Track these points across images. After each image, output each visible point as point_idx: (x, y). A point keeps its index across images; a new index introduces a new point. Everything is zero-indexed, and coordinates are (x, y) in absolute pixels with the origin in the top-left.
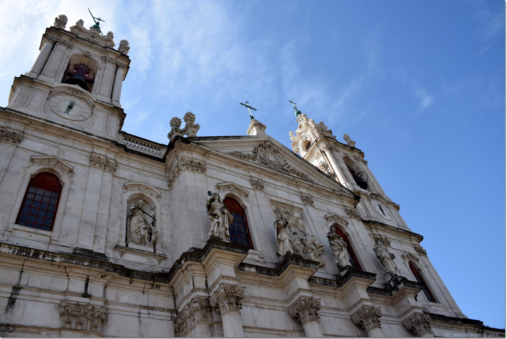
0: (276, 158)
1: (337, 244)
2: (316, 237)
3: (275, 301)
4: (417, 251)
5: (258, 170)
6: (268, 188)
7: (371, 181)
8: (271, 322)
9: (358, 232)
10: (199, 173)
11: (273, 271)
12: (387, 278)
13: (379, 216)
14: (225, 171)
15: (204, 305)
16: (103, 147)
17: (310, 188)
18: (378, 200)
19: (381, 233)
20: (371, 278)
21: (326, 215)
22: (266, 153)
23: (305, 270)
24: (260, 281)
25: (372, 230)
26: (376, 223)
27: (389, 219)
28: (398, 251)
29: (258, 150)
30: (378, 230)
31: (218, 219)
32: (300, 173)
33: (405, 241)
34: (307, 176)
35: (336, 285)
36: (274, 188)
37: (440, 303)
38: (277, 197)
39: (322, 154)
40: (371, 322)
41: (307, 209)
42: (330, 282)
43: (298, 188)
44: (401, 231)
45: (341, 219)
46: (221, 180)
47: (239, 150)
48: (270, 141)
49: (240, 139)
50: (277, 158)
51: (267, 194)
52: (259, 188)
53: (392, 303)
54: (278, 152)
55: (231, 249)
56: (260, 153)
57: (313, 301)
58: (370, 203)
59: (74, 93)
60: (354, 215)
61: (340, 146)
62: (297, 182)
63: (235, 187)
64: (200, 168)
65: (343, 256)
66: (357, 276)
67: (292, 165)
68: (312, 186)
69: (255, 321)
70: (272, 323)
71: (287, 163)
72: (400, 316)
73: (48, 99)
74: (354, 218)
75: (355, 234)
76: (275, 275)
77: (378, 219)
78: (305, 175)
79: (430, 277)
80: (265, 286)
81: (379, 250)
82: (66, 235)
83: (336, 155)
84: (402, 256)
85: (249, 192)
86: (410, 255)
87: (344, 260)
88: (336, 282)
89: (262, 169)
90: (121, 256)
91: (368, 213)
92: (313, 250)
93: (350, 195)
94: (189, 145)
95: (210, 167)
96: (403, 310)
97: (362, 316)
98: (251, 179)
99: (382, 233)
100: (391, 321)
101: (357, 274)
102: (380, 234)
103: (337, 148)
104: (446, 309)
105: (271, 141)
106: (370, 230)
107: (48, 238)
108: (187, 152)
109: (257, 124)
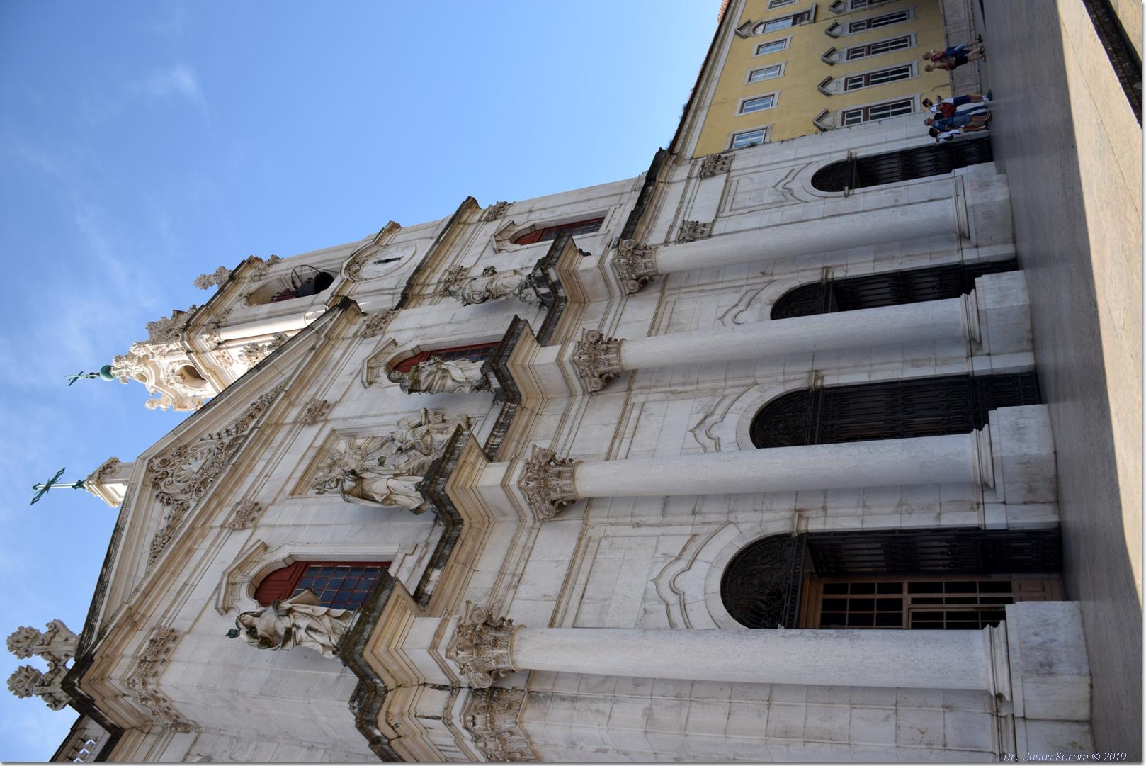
0: (199, 456)
1: (431, 377)
2: (403, 419)
3: (513, 544)
4: (495, 219)
5: (213, 506)
6: (263, 493)
7: (319, 262)
8: (555, 564)
10: (176, 648)
11: (449, 532)
12: (529, 296)
13: (399, 272)
14: (191, 583)
15: (484, 704)
17: (292, 399)
18: (365, 261)
19: (435, 278)
20: (519, 329)
21: (362, 382)
22: (178, 476)
23: (465, 462)
24: (465, 565)
25: (423, 295)
26: (412, 282)
27: (413, 252)
28: (482, 257)
29: (165, 493)
30: (426, 283)
31: (299, 628)
32: (251, 411)
33: (467, 236)
34: (262, 396)
35: (516, 405)
36: (266, 478)
37: (607, 211)
38: (289, 478)
39: (224, 349)
40: (607, 356)
41: (336, 420)
42: (506, 416)
43: (283, 425)
44: (444, 236)
45: (381, 352)
46: (210, 598)
47: (150, 538)
48: (153, 458)
49: (123, 529)
50: (200, 453)
51: (275, 499)
52: (256, 515)
53: (581, 303)
54: (185, 447)
55: (376, 614)
56: (175, 490)
57: (534, 462)
58: (366, 279)
60: (380, 322)
61: (217, 303)
62: (268, 425)
63: (237, 570)
64: (164, 643)
65: (460, 372)
66: (508, 356)
67: (225, 424)
68: (288, 394)
69: (546, 598)
70: (557, 561)
71: (219, 434)
72: (611, 297)
74: (387, 323)
75: (421, 332)
76: (460, 530)
77: (404, 274)
78: (259, 401)
79: (553, 211)
80: (478, 557)
81: (468, 294)
83: (237, 318)
84: (496, 253)
85: (259, 540)
86: (499, 235)
87: (468, 374)
88: (509, 404)
89: (214, 495)
91: (387, 292)
92: (428, 432)
93: (334, 316)
94: (96, 657)
95: (170, 618)
96: (600, 285)
97: (590, 370)
98: (230, 528)
99: (436, 277)
100: (614, 319)
101: (505, 356)
102: (436, 282)
103: (220, 310)
104: (621, 205)
105: (153, 456)
106: (424, 299)
108: (113, 666)
109: (99, 478)
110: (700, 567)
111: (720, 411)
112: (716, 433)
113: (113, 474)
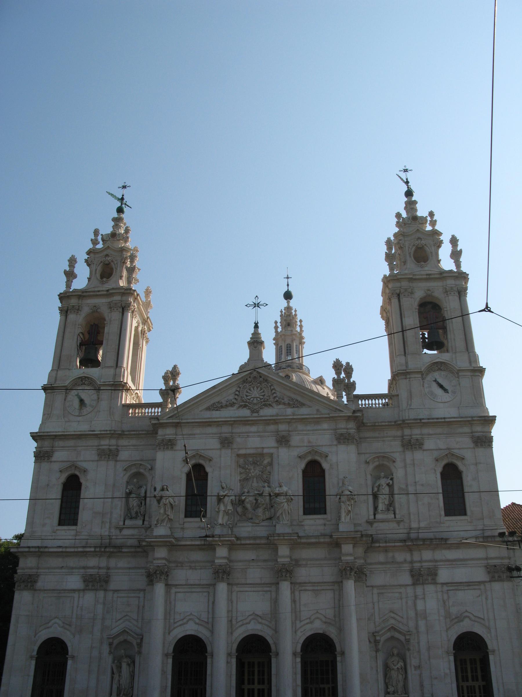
6: (239, 440)
9: (340, 462)
14: (196, 436)
16: (107, 437)
25: (403, 429)
36: (246, 437)
38: (246, 449)
47: (216, 400)
51: (235, 449)
59: (84, 382)
65: (280, 513)
73: (65, 400)
82: (85, 526)
90: (120, 532)
107: (75, 531)
110: (196, 627)
111: (263, 621)
112: (252, 622)
113: (254, 349)
